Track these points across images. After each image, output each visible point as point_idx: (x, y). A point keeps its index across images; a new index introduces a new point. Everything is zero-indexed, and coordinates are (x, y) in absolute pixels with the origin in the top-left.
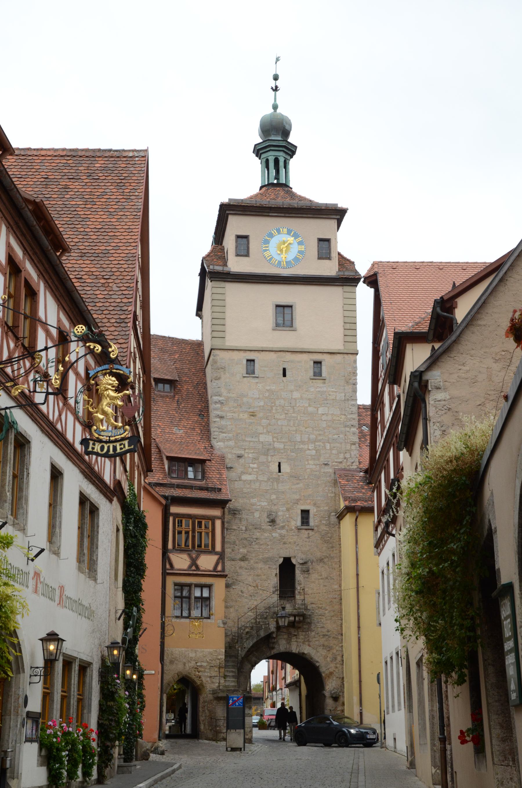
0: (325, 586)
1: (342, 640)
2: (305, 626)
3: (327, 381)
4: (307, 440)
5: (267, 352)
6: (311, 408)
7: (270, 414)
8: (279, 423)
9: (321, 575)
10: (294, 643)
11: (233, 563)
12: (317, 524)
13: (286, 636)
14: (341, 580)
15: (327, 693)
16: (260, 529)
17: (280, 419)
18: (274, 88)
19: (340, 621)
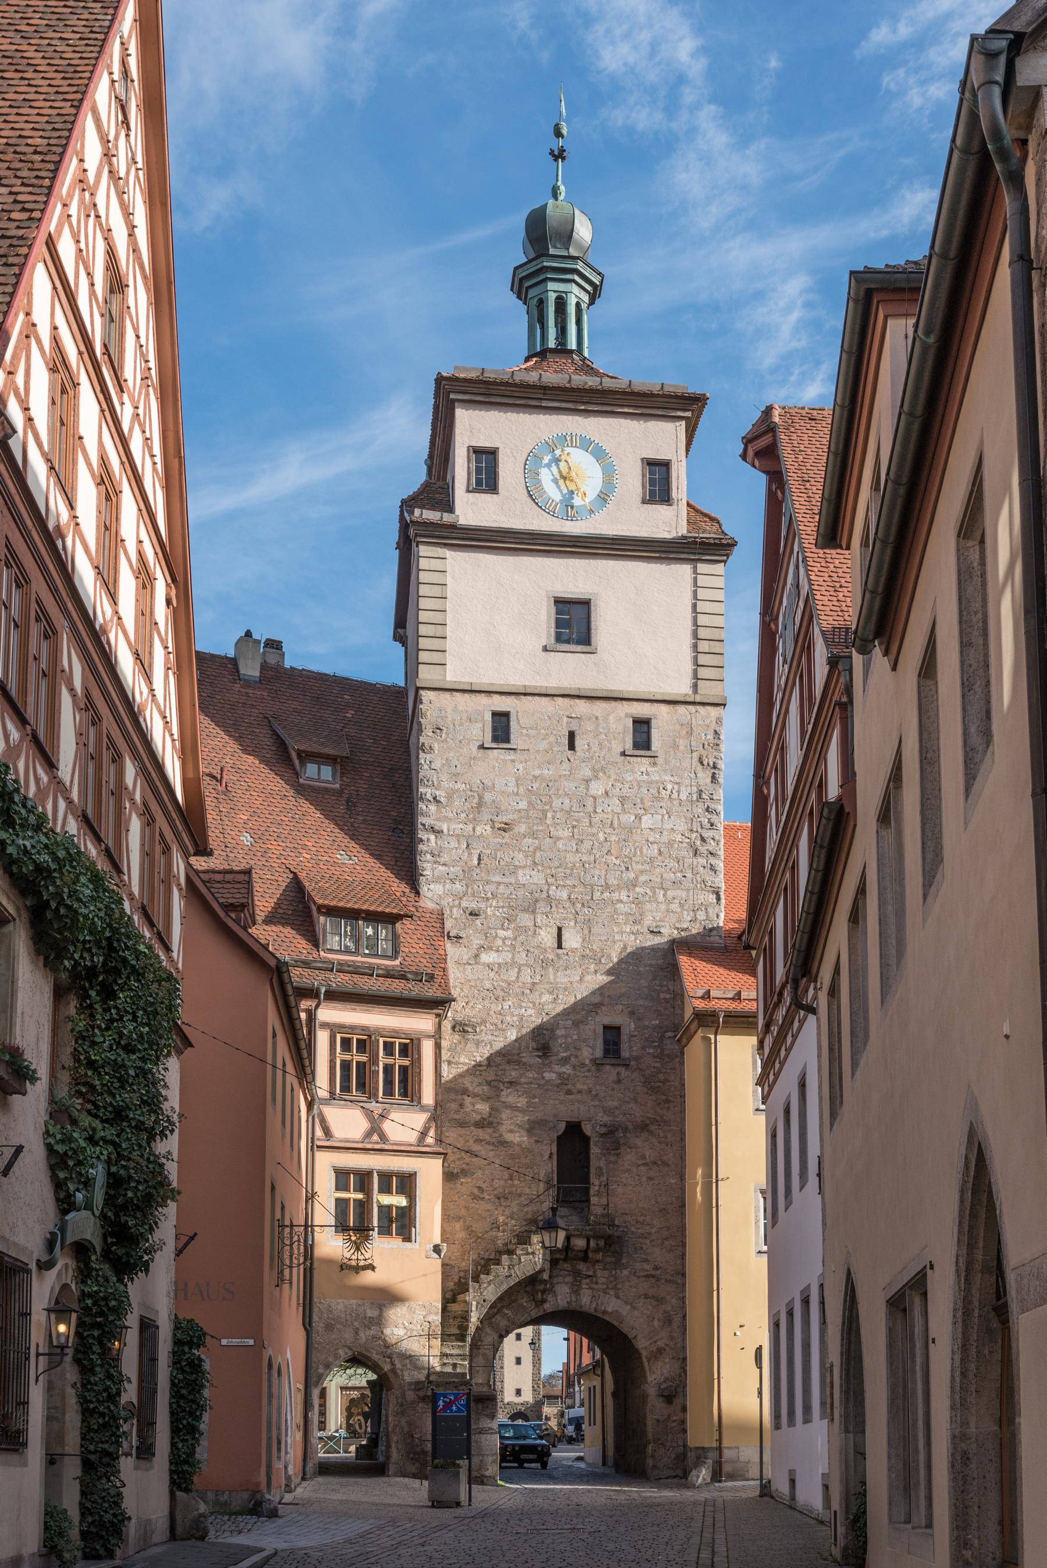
0: (650, 1178)
1: (684, 1285)
2: (608, 1259)
3: (660, 761)
4: (615, 882)
5: (537, 698)
7: (540, 828)
8: (560, 845)
9: (643, 1157)
11: (463, 1131)
12: (634, 1054)
13: (569, 1279)
14: (684, 1167)
15: (652, 1391)
16: (518, 1062)
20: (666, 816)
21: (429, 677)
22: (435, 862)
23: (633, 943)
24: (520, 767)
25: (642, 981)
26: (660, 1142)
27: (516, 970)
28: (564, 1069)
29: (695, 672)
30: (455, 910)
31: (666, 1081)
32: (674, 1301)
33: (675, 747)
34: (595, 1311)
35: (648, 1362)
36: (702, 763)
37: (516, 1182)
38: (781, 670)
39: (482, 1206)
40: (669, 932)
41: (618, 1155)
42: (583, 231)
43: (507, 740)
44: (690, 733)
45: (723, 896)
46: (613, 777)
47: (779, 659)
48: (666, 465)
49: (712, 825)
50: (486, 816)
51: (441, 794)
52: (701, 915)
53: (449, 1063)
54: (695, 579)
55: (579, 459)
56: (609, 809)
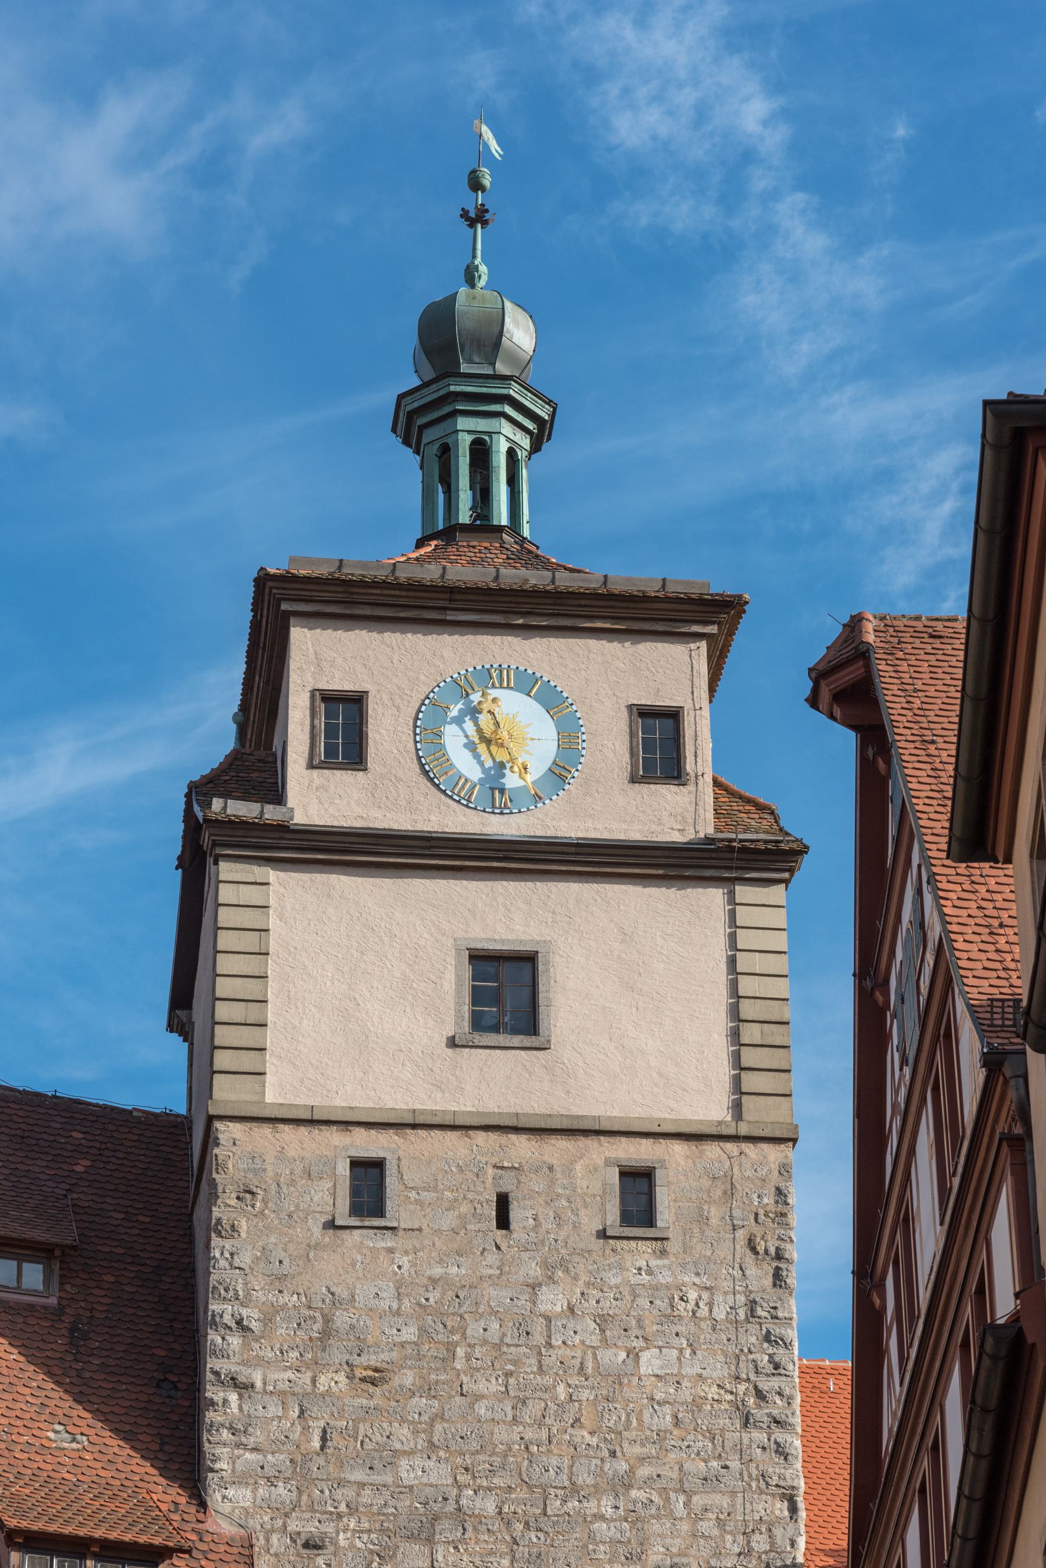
3: (674, 1247)
7: (443, 1377)
8: (481, 1409)
18: (472, 214)
20: (688, 1352)
21: (233, 1097)
22: (239, 1445)
24: (405, 1261)
29: (737, 1081)
30: (275, 1538)
33: (703, 1220)
36: (754, 1250)
38: (897, 1076)
42: (520, 334)
43: (379, 1211)
44: (730, 1193)
45: (801, 1505)
46: (584, 1278)
47: (893, 1057)
48: (674, 715)
49: (777, 1366)
50: (337, 1354)
51: (251, 1315)
52: (760, 1543)
54: (732, 914)
55: (514, 708)
56: (577, 1340)
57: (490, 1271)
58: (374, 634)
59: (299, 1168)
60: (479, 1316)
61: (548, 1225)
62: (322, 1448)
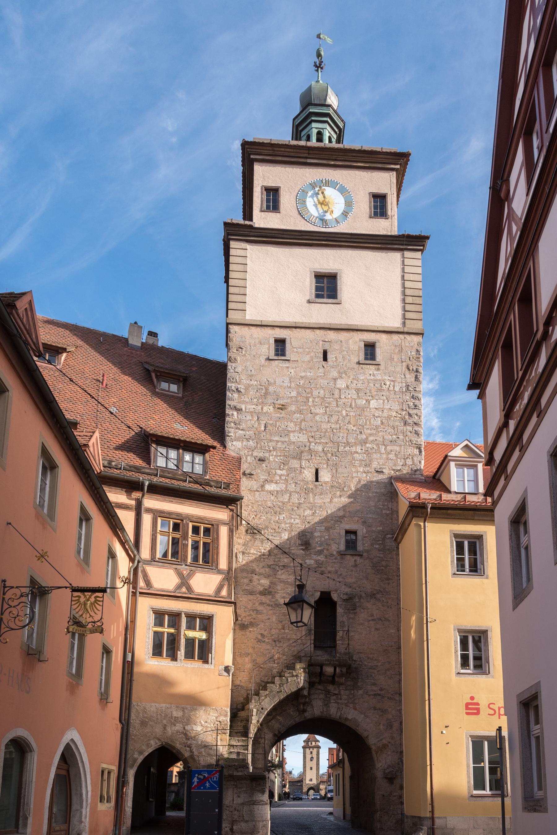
1: (400, 701)
2: (349, 683)
3: (382, 367)
4: (353, 441)
5: (303, 330)
6: (360, 400)
7: (305, 408)
8: (317, 418)
9: (372, 615)
10: (334, 705)
11: (251, 597)
12: (366, 548)
14: (399, 622)
15: (379, 774)
17: (318, 414)
19: (398, 676)
20: (386, 401)
22: (237, 428)
23: (365, 478)
24: (292, 371)
25: (371, 502)
26: (383, 606)
27: (288, 495)
28: (319, 558)
29: (404, 315)
30: (249, 458)
31: (386, 566)
32: (394, 712)
33: (392, 359)
34: (340, 718)
35: (376, 754)
36: (409, 369)
37: (287, 631)
39: (264, 646)
40: (388, 472)
41: (355, 613)
43: (283, 354)
44: (401, 351)
45: (423, 450)
46: (352, 377)
49: (416, 406)
50: (270, 400)
51: (241, 387)
52: (409, 462)
53: (243, 553)
54: (403, 261)
56: (349, 396)
57: (321, 374)
58: (283, 168)
59: (257, 341)
60: (316, 388)
61: (340, 360)
62: (265, 430)
